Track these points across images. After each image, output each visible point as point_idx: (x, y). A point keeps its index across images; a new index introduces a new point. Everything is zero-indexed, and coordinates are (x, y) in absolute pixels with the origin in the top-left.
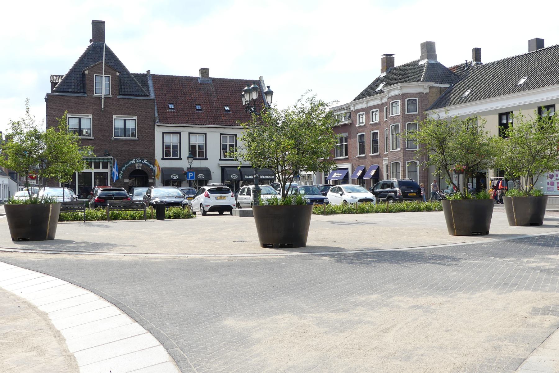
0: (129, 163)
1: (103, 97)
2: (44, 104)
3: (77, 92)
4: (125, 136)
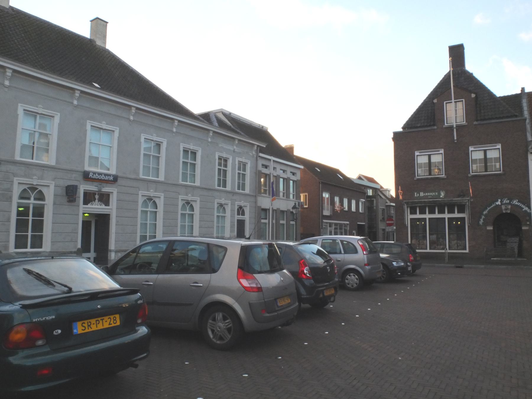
0: (492, 205)
1: (455, 126)
2: (392, 143)
3: (426, 126)
4: (486, 171)
